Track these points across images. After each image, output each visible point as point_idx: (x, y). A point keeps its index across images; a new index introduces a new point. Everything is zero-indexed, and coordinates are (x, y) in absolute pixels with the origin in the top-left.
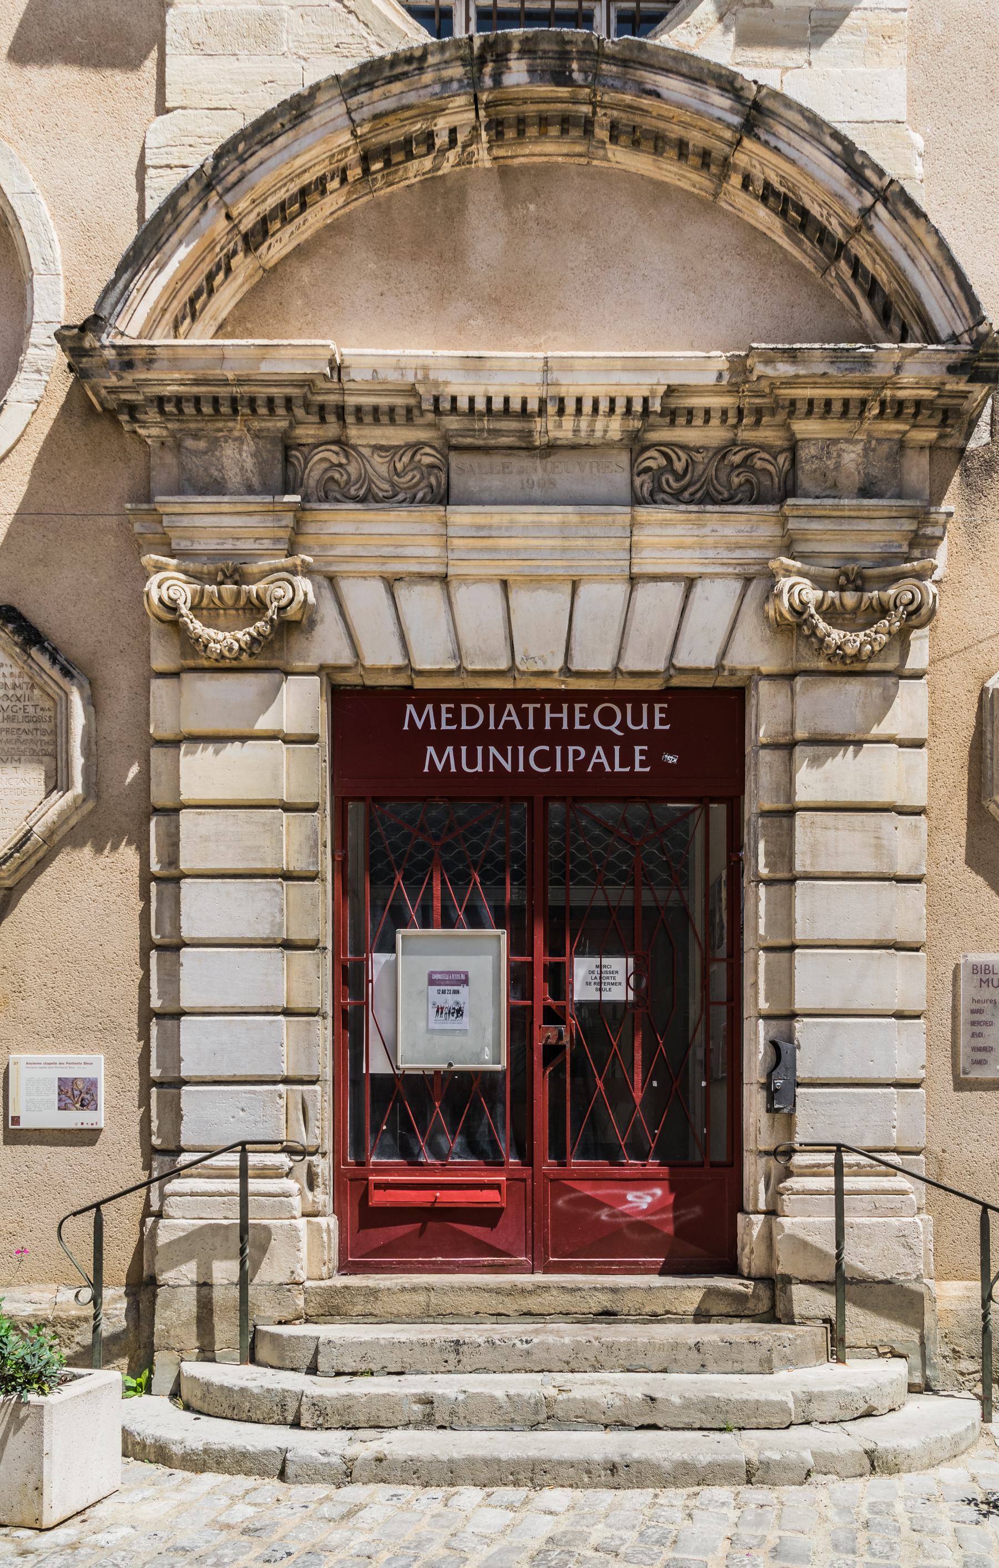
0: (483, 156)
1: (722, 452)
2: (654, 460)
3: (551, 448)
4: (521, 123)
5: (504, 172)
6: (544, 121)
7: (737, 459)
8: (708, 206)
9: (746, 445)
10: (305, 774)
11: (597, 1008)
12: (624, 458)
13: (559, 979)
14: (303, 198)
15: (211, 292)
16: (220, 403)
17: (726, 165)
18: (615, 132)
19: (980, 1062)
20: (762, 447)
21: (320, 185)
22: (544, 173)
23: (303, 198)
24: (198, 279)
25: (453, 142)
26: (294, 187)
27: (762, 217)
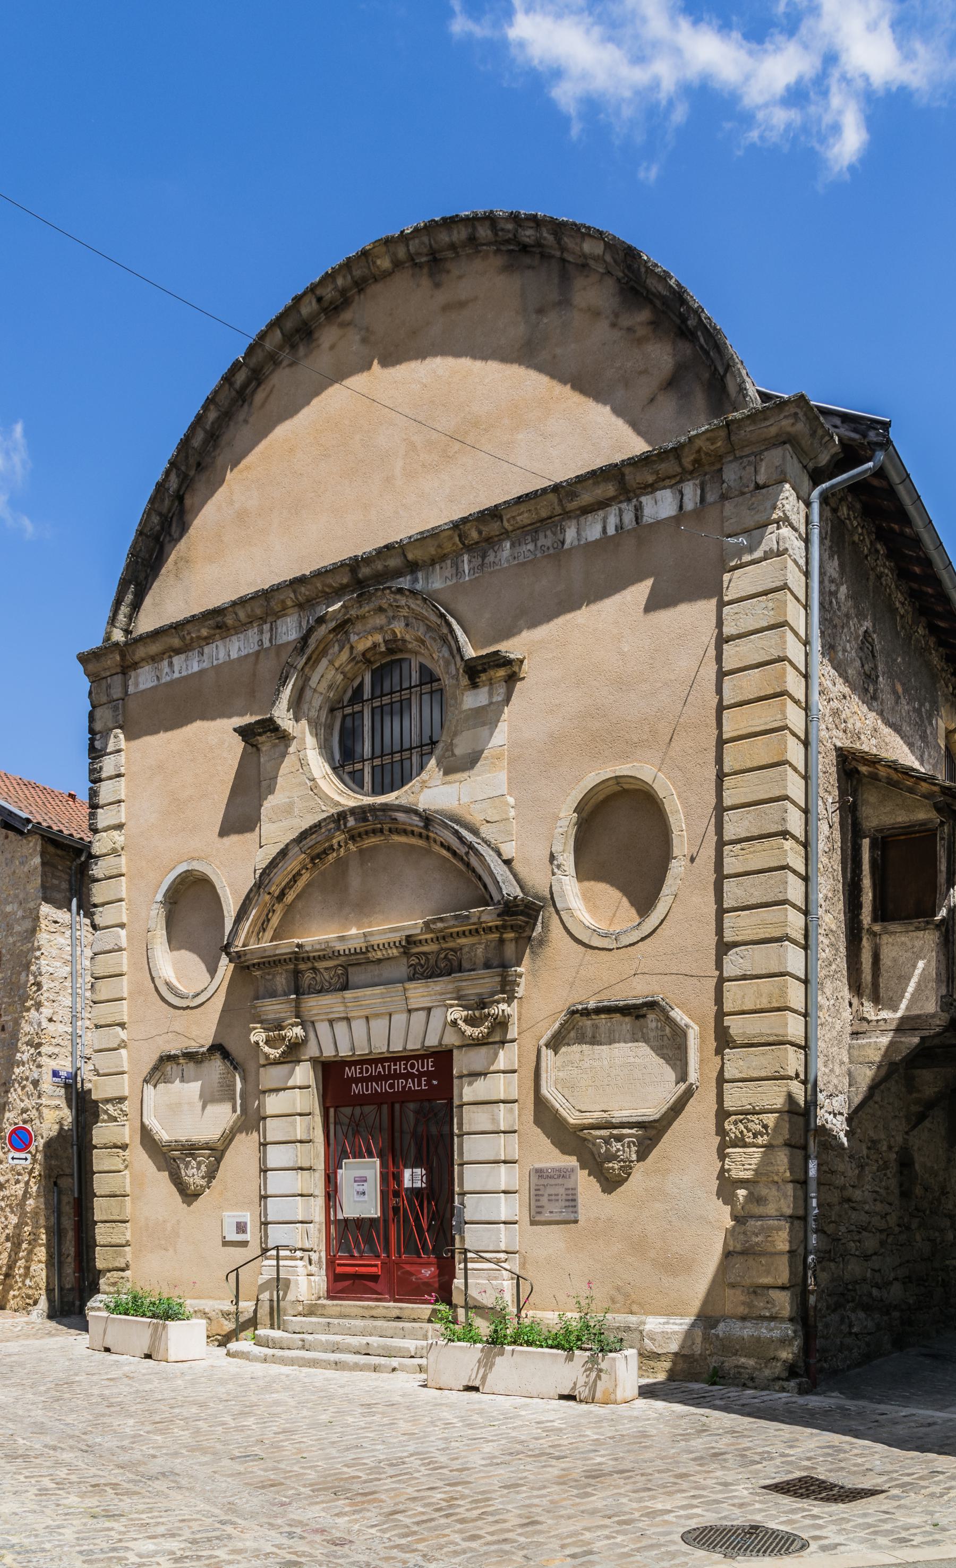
0: (352, 847)
1: (438, 953)
2: (414, 961)
3: (379, 961)
4: (360, 835)
5: (361, 851)
6: (367, 833)
7: (442, 956)
8: (428, 852)
9: (446, 949)
10: (309, 1100)
11: (412, 1189)
12: (405, 960)
13: (398, 1178)
14: (295, 879)
15: (269, 920)
16: (271, 963)
17: (428, 838)
18: (390, 830)
19: (539, 1213)
20: (452, 950)
21: (299, 874)
22: (374, 848)
23: (295, 879)
24: (263, 917)
25: (340, 846)
26: (290, 876)
27: (444, 853)
